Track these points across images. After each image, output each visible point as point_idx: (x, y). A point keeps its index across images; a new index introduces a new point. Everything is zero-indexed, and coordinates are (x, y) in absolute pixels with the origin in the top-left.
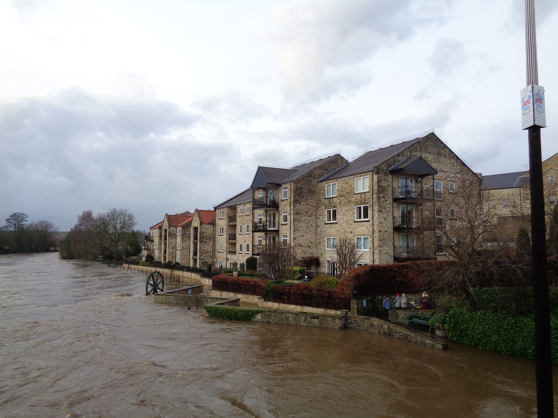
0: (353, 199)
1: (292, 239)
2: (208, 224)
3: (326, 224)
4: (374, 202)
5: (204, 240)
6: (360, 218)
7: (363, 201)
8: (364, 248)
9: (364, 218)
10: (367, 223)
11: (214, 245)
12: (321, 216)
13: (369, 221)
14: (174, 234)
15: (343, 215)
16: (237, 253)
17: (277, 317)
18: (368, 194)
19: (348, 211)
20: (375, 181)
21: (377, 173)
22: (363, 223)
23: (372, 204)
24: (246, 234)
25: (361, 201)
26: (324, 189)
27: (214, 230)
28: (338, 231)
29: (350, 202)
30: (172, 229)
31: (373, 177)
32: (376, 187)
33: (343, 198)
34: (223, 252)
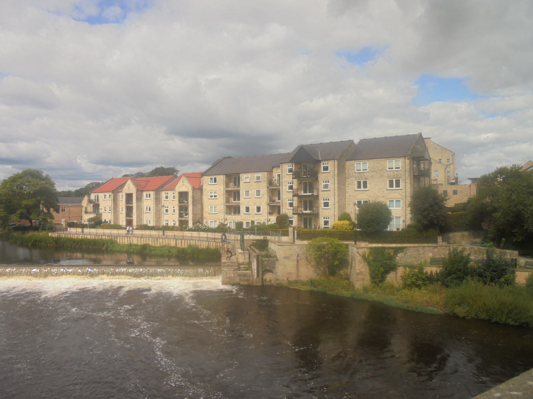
2: (198, 189)
3: (356, 191)
4: (406, 177)
5: (195, 203)
6: (393, 187)
7: (396, 176)
9: (396, 187)
10: (399, 191)
12: (350, 185)
13: (401, 189)
15: (375, 185)
17: (411, 250)
18: (401, 172)
19: (381, 182)
20: (407, 164)
21: (408, 159)
22: (396, 191)
23: (404, 178)
24: (255, 198)
25: (394, 176)
26: (354, 166)
28: (370, 196)
29: (382, 176)
31: (405, 161)
32: (408, 167)
33: (375, 173)
34: (217, 214)
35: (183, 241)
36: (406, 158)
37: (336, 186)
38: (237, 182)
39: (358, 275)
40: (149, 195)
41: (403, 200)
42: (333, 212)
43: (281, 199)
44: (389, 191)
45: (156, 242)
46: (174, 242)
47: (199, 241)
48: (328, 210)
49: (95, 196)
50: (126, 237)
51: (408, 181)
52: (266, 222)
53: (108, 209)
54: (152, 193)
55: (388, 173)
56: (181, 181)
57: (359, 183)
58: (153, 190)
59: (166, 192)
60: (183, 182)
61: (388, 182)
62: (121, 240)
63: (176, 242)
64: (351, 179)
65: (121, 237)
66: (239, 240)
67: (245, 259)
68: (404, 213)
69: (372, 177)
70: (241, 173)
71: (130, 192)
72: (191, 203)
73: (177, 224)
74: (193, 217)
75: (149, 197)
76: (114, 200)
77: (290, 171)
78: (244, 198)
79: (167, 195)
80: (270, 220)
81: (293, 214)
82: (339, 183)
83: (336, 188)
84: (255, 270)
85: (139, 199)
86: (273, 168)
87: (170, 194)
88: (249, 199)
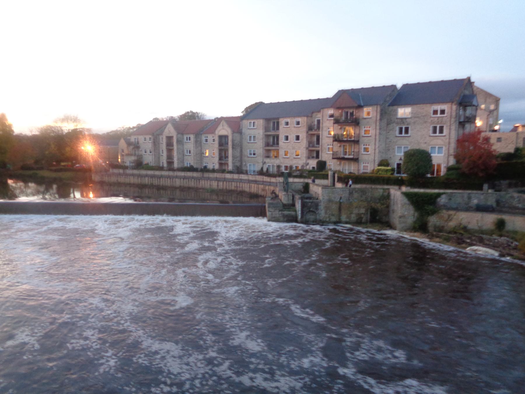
0: (430, 121)
1: (377, 146)
3: (396, 137)
8: (438, 153)
10: (442, 138)
11: (241, 151)
13: (445, 136)
14: (181, 141)
16: (280, 158)
18: (446, 118)
21: (455, 104)
24: (295, 142)
27: (241, 139)
29: (425, 122)
30: (179, 136)
32: (454, 114)
35: (225, 183)
36: (453, 104)
37: (378, 131)
38: (277, 127)
39: (400, 218)
40: (190, 138)
41: (446, 146)
42: (373, 158)
43: (320, 144)
44: (431, 137)
45: (198, 184)
46: (216, 184)
47: (241, 184)
48: (367, 156)
49: (135, 138)
50: (169, 179)
51: (453, 127)
52: (305, 165)
53: (148, 151)
54: (192, 137)
55: (432, 119)
56: (221, 125)
57: (401, 129)
58: (193, 134)
59: (206, 135)
60: (223, 126)
61: (431, 129)
62: (164, 181)
63: (218, 184)
64: (392, 125)
65: (164, 179)
66: (281, 182)
67: (288, 200)
68: (446, 160)
69: (414, 123)
70: (281, 118)
71: (170, 135)
72: (231, 146)
73: (217, 167)
74: (233, 160)
75: (190, 140)
76: (154, 142)
77: (332, 116)
78: (284, 142)
79: (206, 138)
80: (308, 164)
81: (333, 158)
82: (380, 129)
83: (378, 134)
84: (299, 211)
85: (179, 142)
86: (313, 113)
87: (210, 137)
88: (289, 144)
